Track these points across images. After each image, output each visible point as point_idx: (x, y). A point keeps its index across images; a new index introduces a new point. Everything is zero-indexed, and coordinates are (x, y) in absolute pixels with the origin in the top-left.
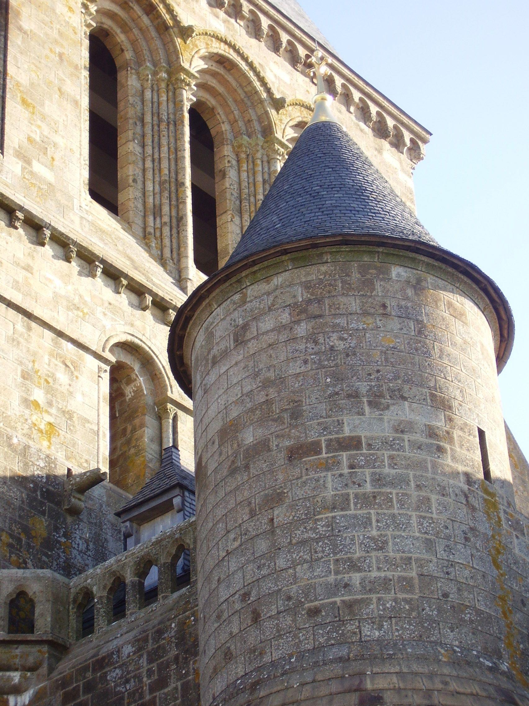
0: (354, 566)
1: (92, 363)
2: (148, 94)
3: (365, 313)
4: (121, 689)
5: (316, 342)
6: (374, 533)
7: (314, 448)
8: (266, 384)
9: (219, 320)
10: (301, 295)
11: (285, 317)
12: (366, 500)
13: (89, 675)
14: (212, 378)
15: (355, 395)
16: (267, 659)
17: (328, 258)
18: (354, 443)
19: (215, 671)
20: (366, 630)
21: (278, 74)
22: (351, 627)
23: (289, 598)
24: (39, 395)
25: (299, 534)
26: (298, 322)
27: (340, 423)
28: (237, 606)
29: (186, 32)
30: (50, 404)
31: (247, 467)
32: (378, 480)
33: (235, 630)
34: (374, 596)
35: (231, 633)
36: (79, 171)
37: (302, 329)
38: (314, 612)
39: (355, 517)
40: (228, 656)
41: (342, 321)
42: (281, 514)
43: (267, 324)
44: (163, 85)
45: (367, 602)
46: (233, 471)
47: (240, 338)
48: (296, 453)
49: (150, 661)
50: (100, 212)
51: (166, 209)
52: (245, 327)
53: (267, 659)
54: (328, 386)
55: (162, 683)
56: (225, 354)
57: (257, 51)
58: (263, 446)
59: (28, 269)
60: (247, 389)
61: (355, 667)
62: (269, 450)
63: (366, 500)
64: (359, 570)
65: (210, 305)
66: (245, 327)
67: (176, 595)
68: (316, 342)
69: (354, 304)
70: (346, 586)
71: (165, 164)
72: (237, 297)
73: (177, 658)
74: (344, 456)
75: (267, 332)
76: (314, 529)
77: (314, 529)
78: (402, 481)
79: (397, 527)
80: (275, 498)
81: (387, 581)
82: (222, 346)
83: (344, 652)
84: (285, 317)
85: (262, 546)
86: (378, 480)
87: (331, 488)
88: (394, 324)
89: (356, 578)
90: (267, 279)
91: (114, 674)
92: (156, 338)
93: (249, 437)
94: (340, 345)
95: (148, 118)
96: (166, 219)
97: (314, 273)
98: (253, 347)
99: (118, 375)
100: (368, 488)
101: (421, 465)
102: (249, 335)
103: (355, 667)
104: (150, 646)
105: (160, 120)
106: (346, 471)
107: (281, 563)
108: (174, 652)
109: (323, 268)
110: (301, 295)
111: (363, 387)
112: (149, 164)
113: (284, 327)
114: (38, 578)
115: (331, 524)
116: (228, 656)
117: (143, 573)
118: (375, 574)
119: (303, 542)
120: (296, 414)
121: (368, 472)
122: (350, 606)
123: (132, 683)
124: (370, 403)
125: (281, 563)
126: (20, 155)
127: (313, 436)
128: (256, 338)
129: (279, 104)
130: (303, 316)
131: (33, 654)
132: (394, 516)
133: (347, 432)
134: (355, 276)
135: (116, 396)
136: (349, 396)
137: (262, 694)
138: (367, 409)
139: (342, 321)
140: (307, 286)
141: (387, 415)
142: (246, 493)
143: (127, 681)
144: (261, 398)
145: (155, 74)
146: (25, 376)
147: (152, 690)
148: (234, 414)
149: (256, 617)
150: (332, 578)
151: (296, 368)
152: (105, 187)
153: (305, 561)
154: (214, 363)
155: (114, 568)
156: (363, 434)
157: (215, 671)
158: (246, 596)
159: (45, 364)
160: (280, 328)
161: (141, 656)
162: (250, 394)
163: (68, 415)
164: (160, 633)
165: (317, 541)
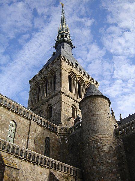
9: (84, 103)
19: (85, 136)
21: (86, 79)
24: (66, 110)
29: (77, 75)
32: (99, 118)
36: (68, 89)
37: (92, 104)
38: (94, 130)
40: (86, 135)
42: (90, 121)
47: (86, 104)
50: (70, 93)
57: (84, 77)
58: (88, 115)
61: (98, 136)
85: (89, 124)
92: (77, 105)
98: (87, 106)
99: (73, 107)
103: (98, 136)
116: (86, 135)
126: (63, 87)
129: (86, 82)
131: (67, 134)
133: (96, 113)
135: (72, 110)
146: (64, 108)
152: (71, 90)
156: (98, 114)
159: (66, 107)
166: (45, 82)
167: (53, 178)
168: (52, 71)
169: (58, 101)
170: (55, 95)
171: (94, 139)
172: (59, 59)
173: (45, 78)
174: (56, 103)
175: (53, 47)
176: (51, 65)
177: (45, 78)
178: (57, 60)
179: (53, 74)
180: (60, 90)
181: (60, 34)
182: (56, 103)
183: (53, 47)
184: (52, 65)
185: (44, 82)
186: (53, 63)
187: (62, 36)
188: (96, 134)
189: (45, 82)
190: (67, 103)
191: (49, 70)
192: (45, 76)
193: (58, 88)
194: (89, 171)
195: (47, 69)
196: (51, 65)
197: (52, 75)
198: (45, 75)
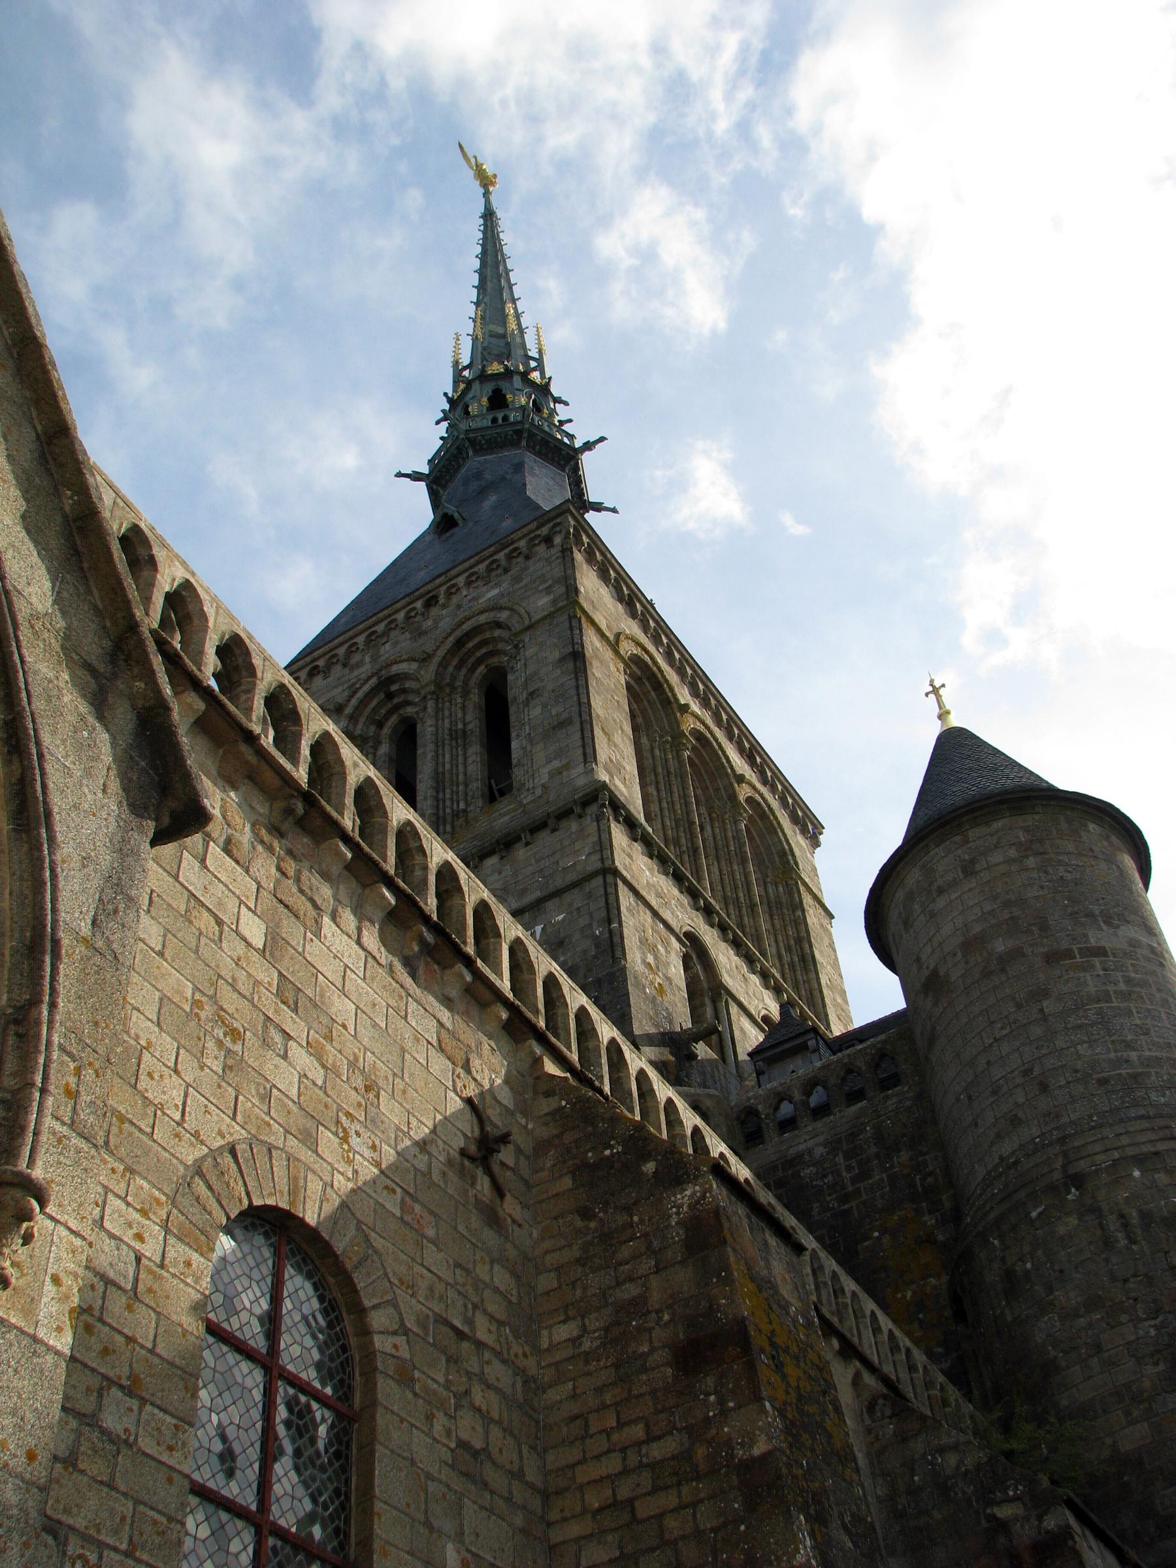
0: (1128, 1046)
1: (676, 944)
2: (657, 752)
3: (1080, 854)
4: (820, 1183)
5: (1046, 872)
6: (1138, 1022)
7: (1069, 954)
8: (1007, 904)
10: (1023, 837)
11: (1013, 853)
12: (1126, 996)
13: (780, 1173)
14: (941, 903)
15: (1090, 915)
16: (1065, 1119)
17: (1040, 809)
18: (1100, 952)
20: (1153, 1096)
22: (1140, 1093)
23: (1076, 1071)
25: (1072, 1020)
26: (1027, 857)
27: (1086, 936)
28: (1019, 1080)
30: (658, 968)
31: (1003, 970)
32: (1128, 981)
33: (1021, 1100)
34: (1152, 1071)
35: (1016, 1103)
37: (1031, 862)
38: (1103, 1082)
39: (1118, 1008)
41: (1065, 858)
42: (1048, 1005)
43: (996, 857)
44: (668, 746)
45: (1148, 1074)
46: (987, 974)
47: (968, 869)
48: (1053, 958)
49: (847, 1156)
51: (683, 841)
52: (973, 861)
53: (1065, 1119)
54: (1067, 906)
55: (864, 1175)
56: (955, 883)
57: (720, 735)
58: (1016, 954)
59: (630, 856)
60: (988, 907)
62: (1024, 955)
63: (1126, 996)
64: (1134, 1050)
65: (927, 845)
66: (973, 861)
67: (854, 1108)
68: (1046, 872)
69: (1070, 847)
70: (1127, 1061)
71: (678, 806)
72: (957, 838)
73: (877, 1155)
74: (1096, 961)
75: (998, 864)
76: (1087, 1017)
77: (1087, 1017)
78: (1144, 984)
79: (1153, 1018)
80: (1044, 993)
81: (1159, 1059)
82: (949, 877)
83: (1142, 1112)
84: (1013, 853)
86: (1128, 981)
87: (1092, 987)
88: (1103, 865)
89: (1133, 1055)
90: (987, 824)
91: (808, 1171)
93: (1000, 946)
94: (1069, 876)
95: (660, 770)
96: (684, 848)
97: (1029, 820)
100: (1122, 986)
101: (1153, 973)
102: (978, 867)
103: (1160, 1122)
104: (845, 1147)
105: (669, 773)
106: (1101, 973)
107: (1060, 1043)
108: (873, 1150)
109: (1037, 817)
110: (1023, 837)
111: (1096, 910)
112: (665, 805)
113: (1014, 860)
114: (709, 1096)
115: (1100, 1012)
116: (1015, 1122)
117: (808, 1094)
118: (1147, 1053)
119: (1080, 1027)
120: (1044, 927)
121: (1119, 974)
122: (1135, 1076)
123: (830, 1177)
124: (1105, 922)
125: (1060, 1043)
127: (1065, 945)
128: (988, 868)
130: (1030, 853)
132: (1148, 1010)
133: (1093, 942)
134: (1064, 825)
136: (1086, 916)
137: (1076, 1144)
138: (1104, 927)
139: (1065, 858)
140: (1026, 830)
141: (1120, 932)
142: (1008, 991)
143: (825, 1176)
144: (1006, 915)
145: (661, 737)
147: (854, 1180)
148: (977, 929)
149: (1044, 1087)
150: (1112, 1055)
151: (1032, 892)
153: (1085, 1042)
154: (941, 891)
155: (780, 1089)
156: (1107, 945)
157: (999, 1136)
158: (1027, 1072)
160: (1009, 861)
161: (836, 1155)
162: (992, 913)
163: (668, 979)
164: (852, 1136)
165: (1092, 1025)
166: (386, 730)
167: (918, 1446)
168: (468, 635)
169: (571, 877)
170: (537, 828)
171: (1130, 1152)
172: (548, 540)
173: (390, 696)
174: (558, 893)
175: (416, 477)
176: (461, 580)
177: (390, 696)
178: (531, 545)
179: (479, 662)
180: (581, 782)
181: (483, 377)
182: (558, 893)
183: (416, 477)
184: (469, 583)
185: (380, 725)
186: (482, 567)
187: (498, 401)
188: (1133, 1113)
189: (386, 730)
190: (653, 902)
191: (443, 621)
192: (391, 679)
193: (567, 767)
194: (1132, 1437)
195: (408, 618)
196: (461, 580)
197: (473, 669)
198: (395, 669)
